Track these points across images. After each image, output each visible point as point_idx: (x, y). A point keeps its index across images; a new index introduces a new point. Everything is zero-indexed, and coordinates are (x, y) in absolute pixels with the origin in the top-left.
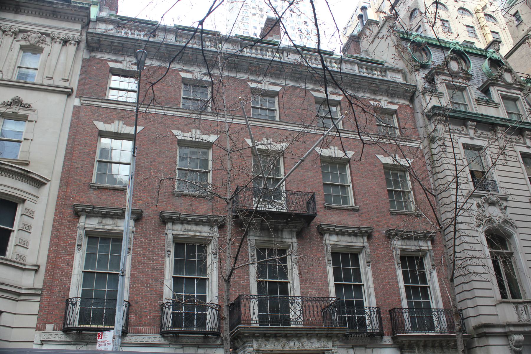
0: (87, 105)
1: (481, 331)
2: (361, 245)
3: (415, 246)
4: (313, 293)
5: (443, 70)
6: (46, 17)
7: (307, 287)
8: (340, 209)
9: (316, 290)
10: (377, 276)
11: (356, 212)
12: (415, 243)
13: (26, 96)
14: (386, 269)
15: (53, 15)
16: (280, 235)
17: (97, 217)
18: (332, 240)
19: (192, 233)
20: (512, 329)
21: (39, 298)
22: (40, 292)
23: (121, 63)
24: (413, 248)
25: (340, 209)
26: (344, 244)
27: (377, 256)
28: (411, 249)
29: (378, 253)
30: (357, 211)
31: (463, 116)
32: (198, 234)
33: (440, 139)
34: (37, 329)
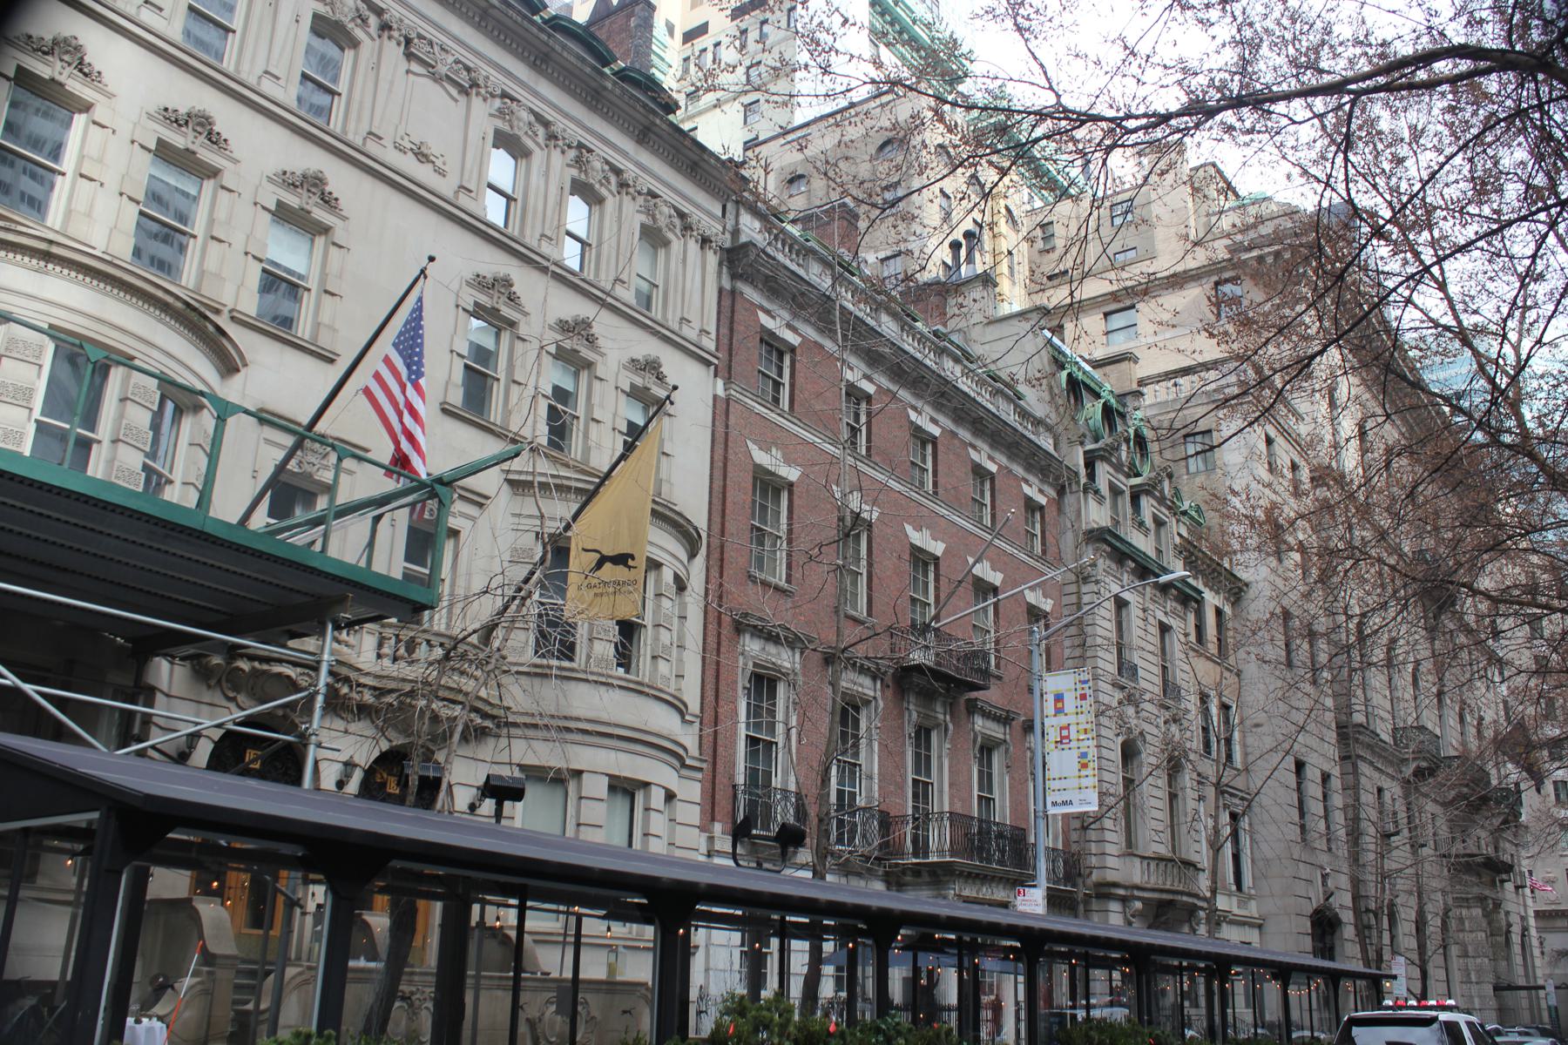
0: (737, 401)
1: (1105, 890)
2: (1001, 736)
4: (959, 809)
5: (1111, 454)
6: (678, 170)
13: (340, 178)
15: (482, 19)
17: (760, 637)
18: (979, 723)
20: (1136, 893)
21: (699, 775)
22: (704, 765)
23: (773, 317)
31: (1127, 551)
33: (1097, 582)
34: (702, 829)
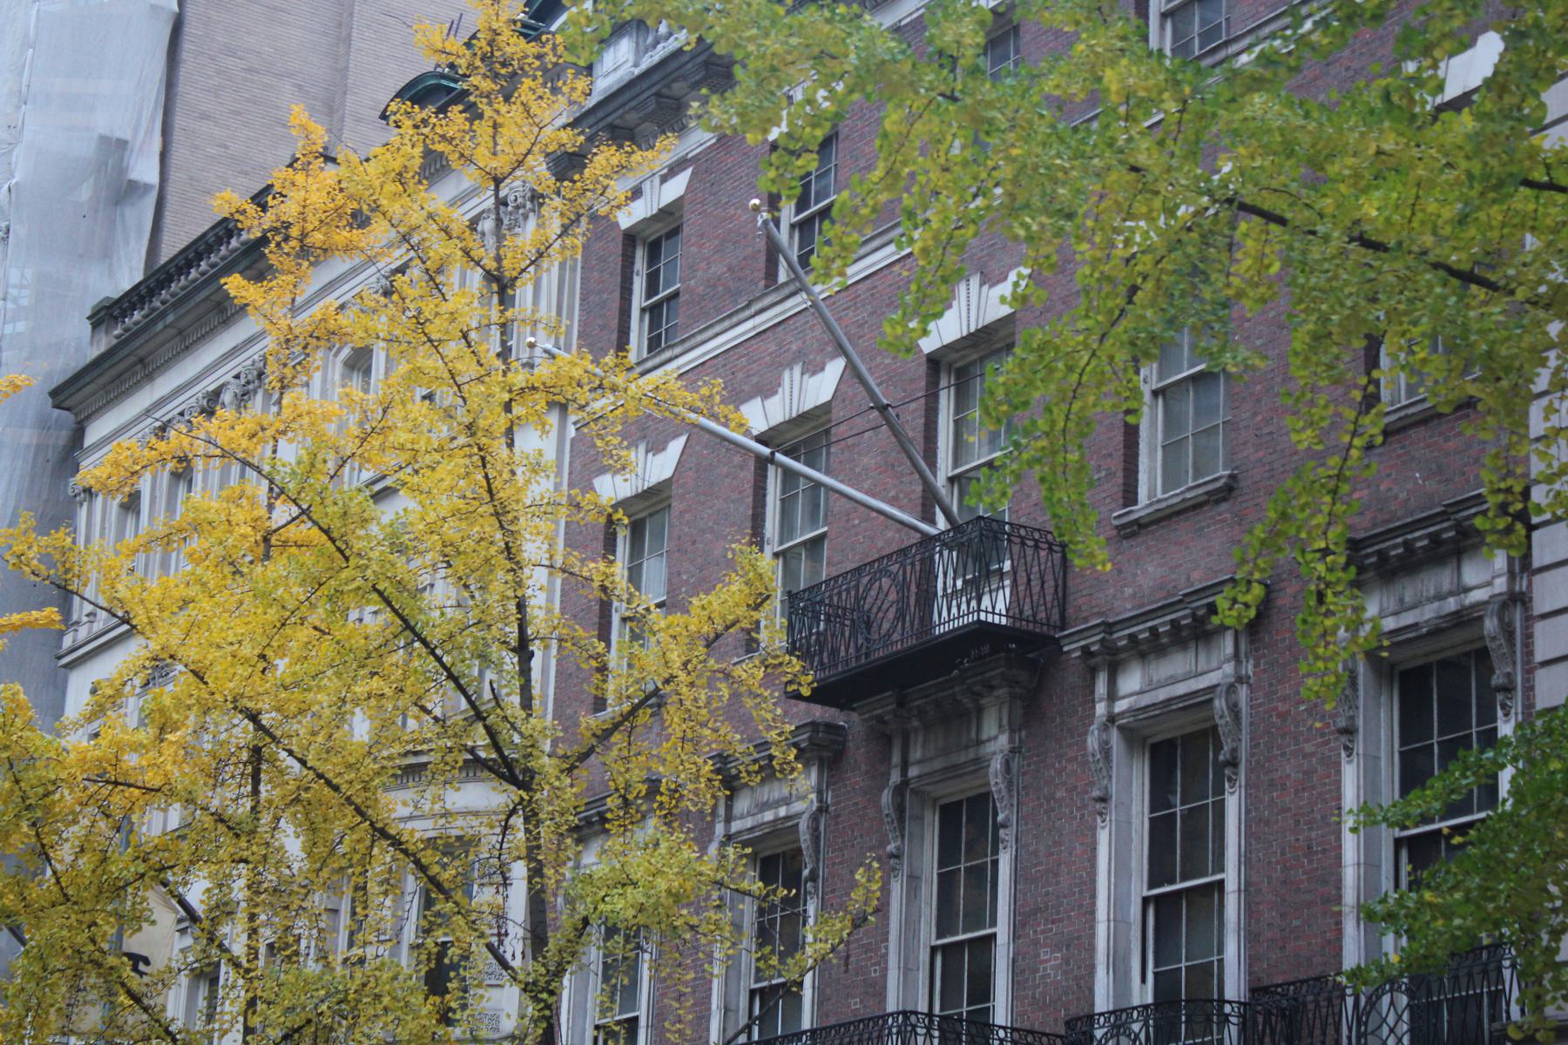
3: (1440, 597)
7: (1036, 943)
8: (1169, 517)
9: (1060, 950)
10: (1267, 823)
11: (1224, 506)
12: (1443, 578)
14: (1305, 773)
16: (973, 735)
19: (769, 816)
24: (1428, 613)
25: (1169, 517)
26: (1162, 695)
27: (1280, 715)
28: (1415, 626)
29: (1284, 699)
30: (1225, 499)
32: (782, 812)
